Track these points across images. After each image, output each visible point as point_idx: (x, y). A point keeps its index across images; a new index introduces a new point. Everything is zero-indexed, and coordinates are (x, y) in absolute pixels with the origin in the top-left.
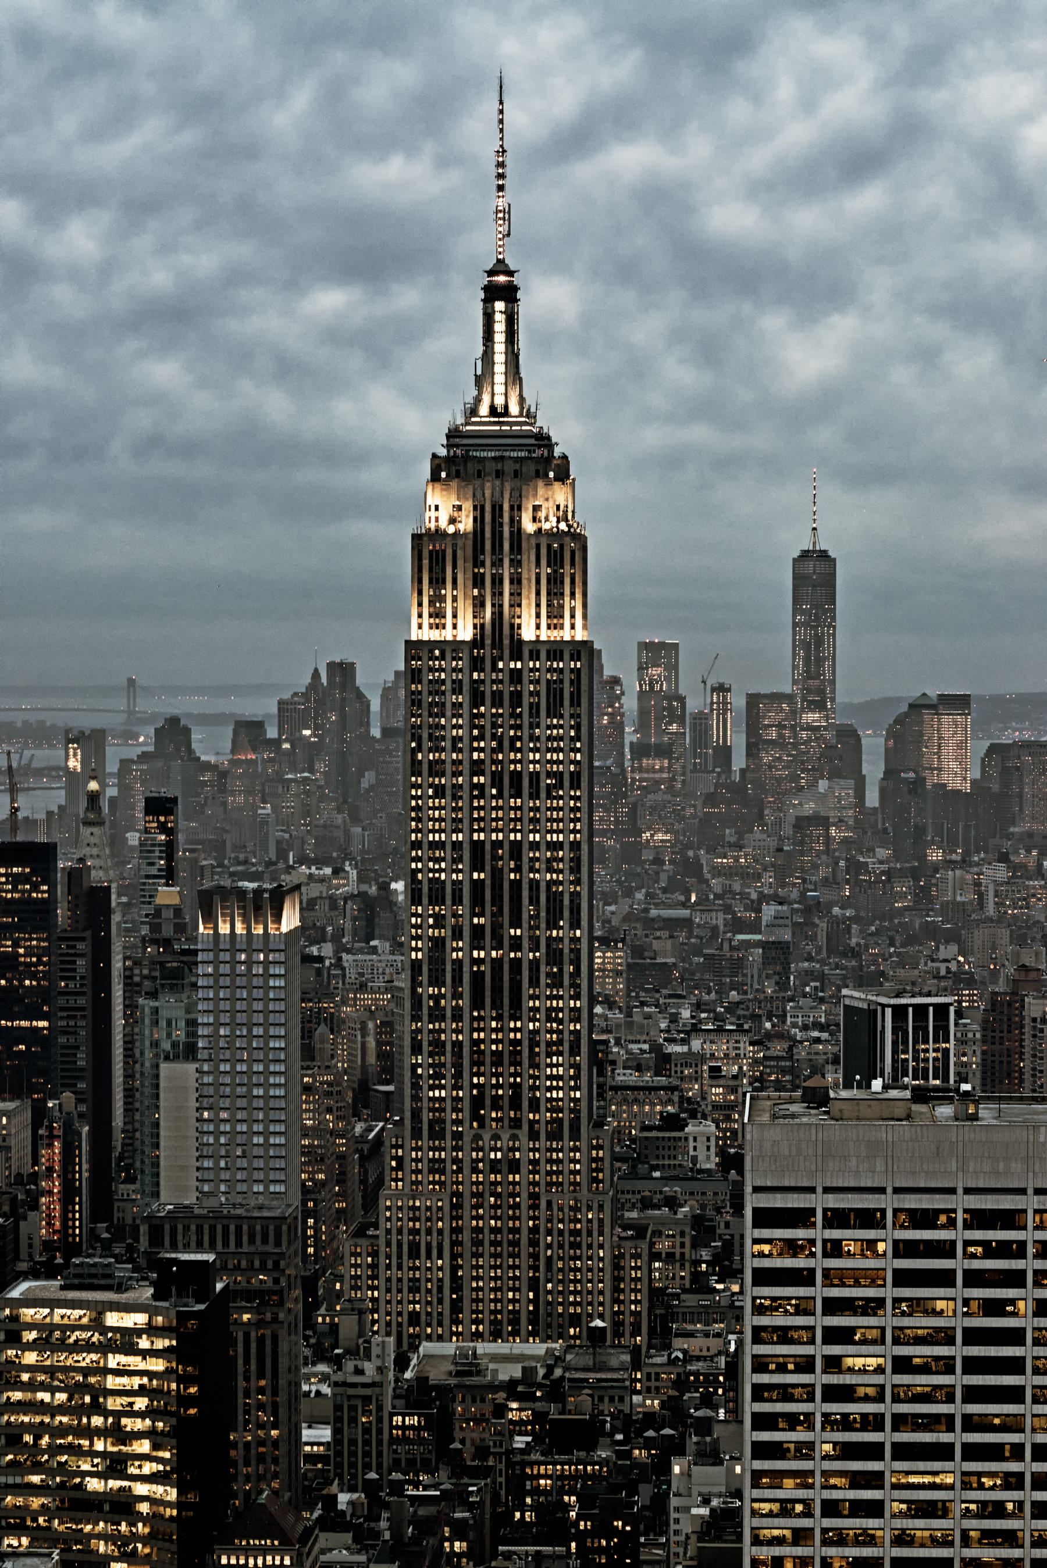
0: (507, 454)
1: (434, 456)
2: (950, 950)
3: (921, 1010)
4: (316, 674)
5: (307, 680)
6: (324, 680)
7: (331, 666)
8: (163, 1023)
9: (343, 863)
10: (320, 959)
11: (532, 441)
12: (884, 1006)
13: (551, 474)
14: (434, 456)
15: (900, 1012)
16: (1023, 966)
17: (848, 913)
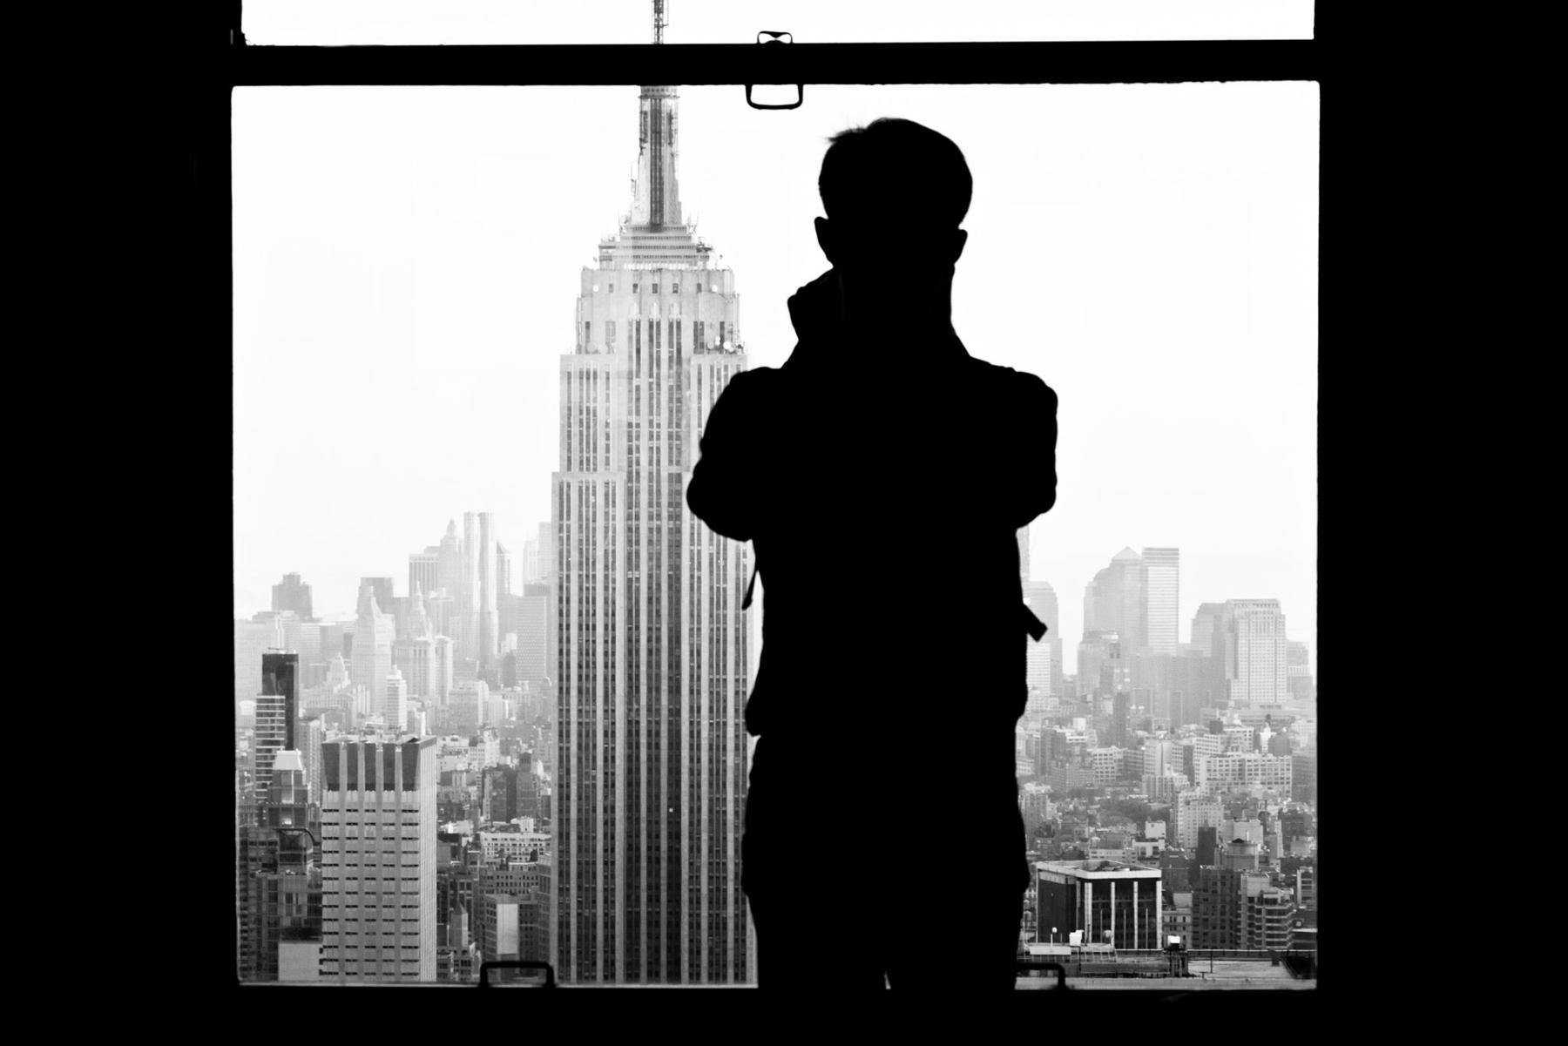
0: (664, 266)
1: (585, 269)
2: (1156, 829)
3: (1124, 885)
4: (452, 524)
5: (443, 532)
6: (460, 532)
7: (468, 516)
8: (283, 899)
9: (482, 734)
10: (456, 838)
11: (694, 252)
12: (1083, 881)
13: (715, 288)
14: (585, 269)
15: (1101, 887)
16: (1239, 841)
17: (1044, 789)
